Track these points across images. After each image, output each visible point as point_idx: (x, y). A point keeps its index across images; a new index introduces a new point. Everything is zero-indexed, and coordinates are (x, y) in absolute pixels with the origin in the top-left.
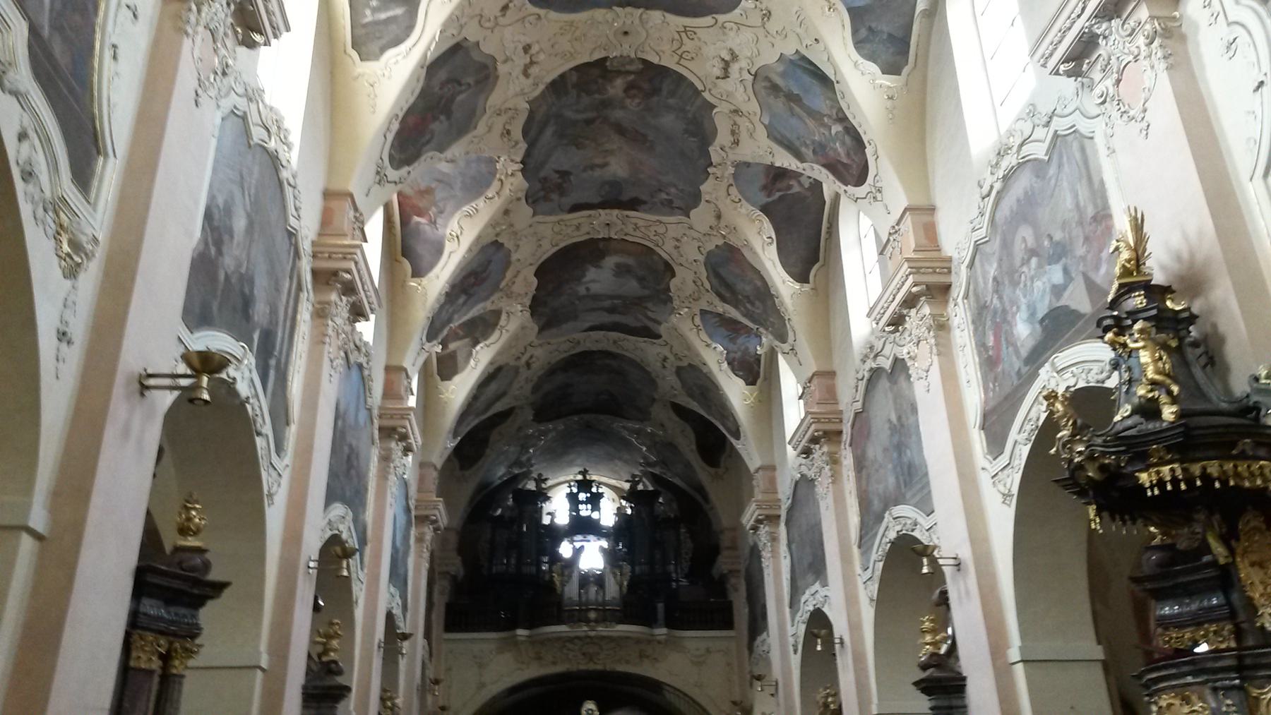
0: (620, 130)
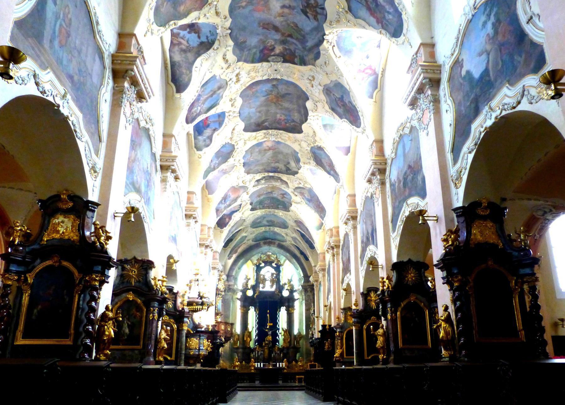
0: (276, 29)
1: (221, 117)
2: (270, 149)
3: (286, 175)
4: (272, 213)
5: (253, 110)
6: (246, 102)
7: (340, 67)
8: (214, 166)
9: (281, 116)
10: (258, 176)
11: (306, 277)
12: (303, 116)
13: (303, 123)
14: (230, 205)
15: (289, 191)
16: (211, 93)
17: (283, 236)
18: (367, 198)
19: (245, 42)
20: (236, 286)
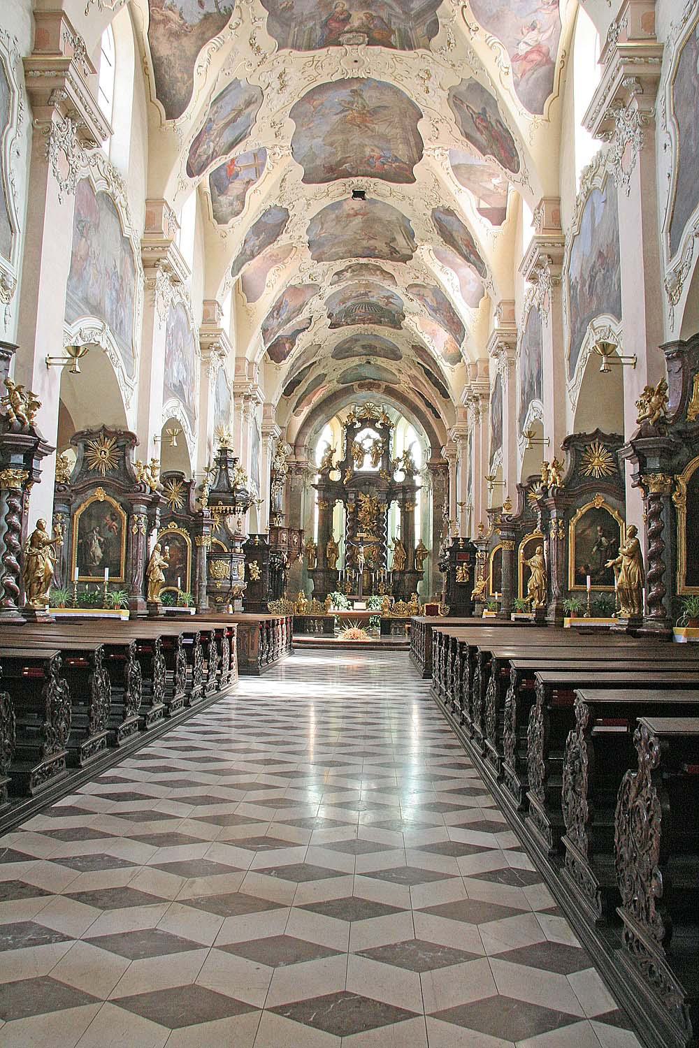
1: (260, 155)
5: (319, 141)
6: (302, 126)
7: (477, 50)
10: (339, 265)
11: (436, 448)
14: (289, 320)
15: (398, 291)
18: (532, 308)
19: (292, 7)
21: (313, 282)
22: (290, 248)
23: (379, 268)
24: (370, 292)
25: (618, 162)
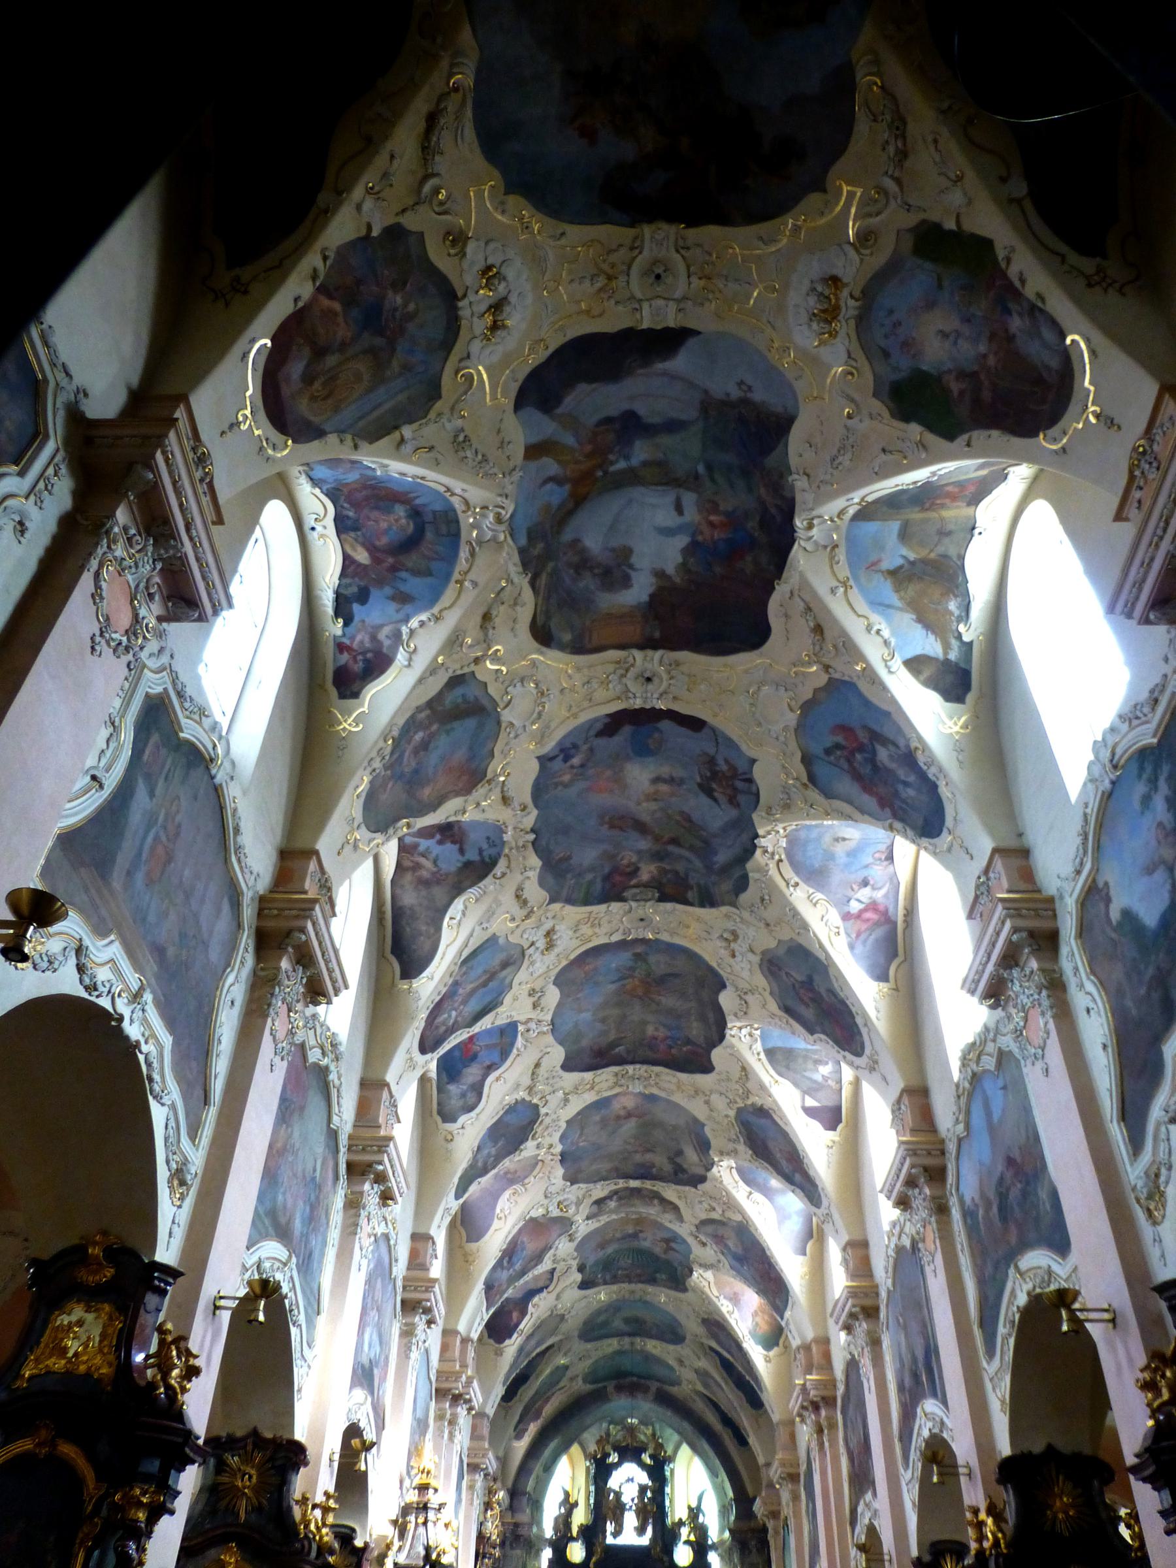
0: (641, 827)
1: (507, 1035)
2: (629, 1115)
3: (674, 1186)
4: (637, 1297)
5: (587, 1016)
6: (569, 996)
8: (485, 1164)
9: (657, 1029)
10: (600, 1190)
12: (714, 1028)
13: (715, 1046)
14: (523, 1273)
15: (684, 1230)
16: (484, 978)
17: (671, 1369)
18: (899, 1250)
19: (570, 858)
20: (535, 1530)
21: (560, 1214)
22: (535, 1162)
23: (657, 1196)
24: (641, 1231)
25: (1021, 1034)
